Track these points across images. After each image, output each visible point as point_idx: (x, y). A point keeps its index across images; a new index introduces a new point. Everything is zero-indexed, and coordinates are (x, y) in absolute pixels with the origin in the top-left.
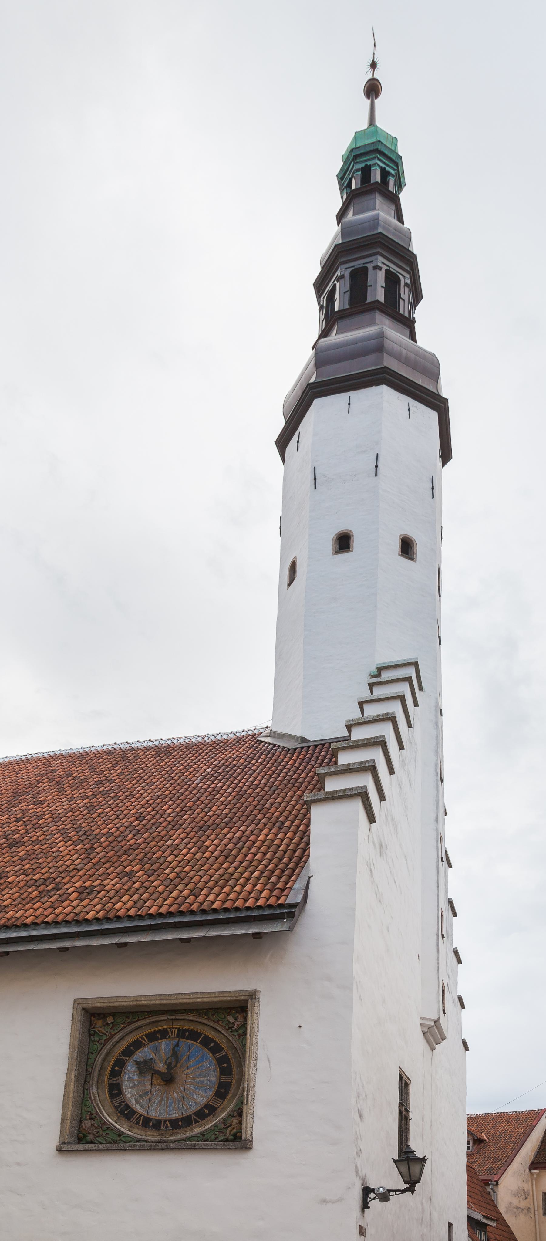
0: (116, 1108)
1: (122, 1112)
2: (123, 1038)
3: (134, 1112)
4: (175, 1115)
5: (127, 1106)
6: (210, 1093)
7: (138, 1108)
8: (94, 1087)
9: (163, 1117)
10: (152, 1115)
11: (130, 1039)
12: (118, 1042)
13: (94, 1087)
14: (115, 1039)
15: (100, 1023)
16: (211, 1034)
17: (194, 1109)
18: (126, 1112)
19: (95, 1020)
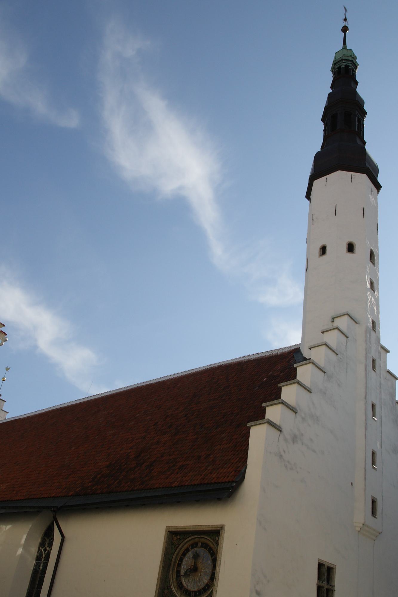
0: (178, 583)
1: (179, 586)
2: (183, 547)
3: (183, 586)
4: (196, 589)
5: (181, 583)
6: (209, 578)
7: (184, 584)
8: (171, 572)
9: (192, 589)
10: (189, 588)
11: (185, 547)
12: (181, 548)
13: (171, 572)
14: (180, 547)
15: (175, 538)
16: (212, 545)
17: (202, 586)
18: (180, 586)
19: (175, 536)
